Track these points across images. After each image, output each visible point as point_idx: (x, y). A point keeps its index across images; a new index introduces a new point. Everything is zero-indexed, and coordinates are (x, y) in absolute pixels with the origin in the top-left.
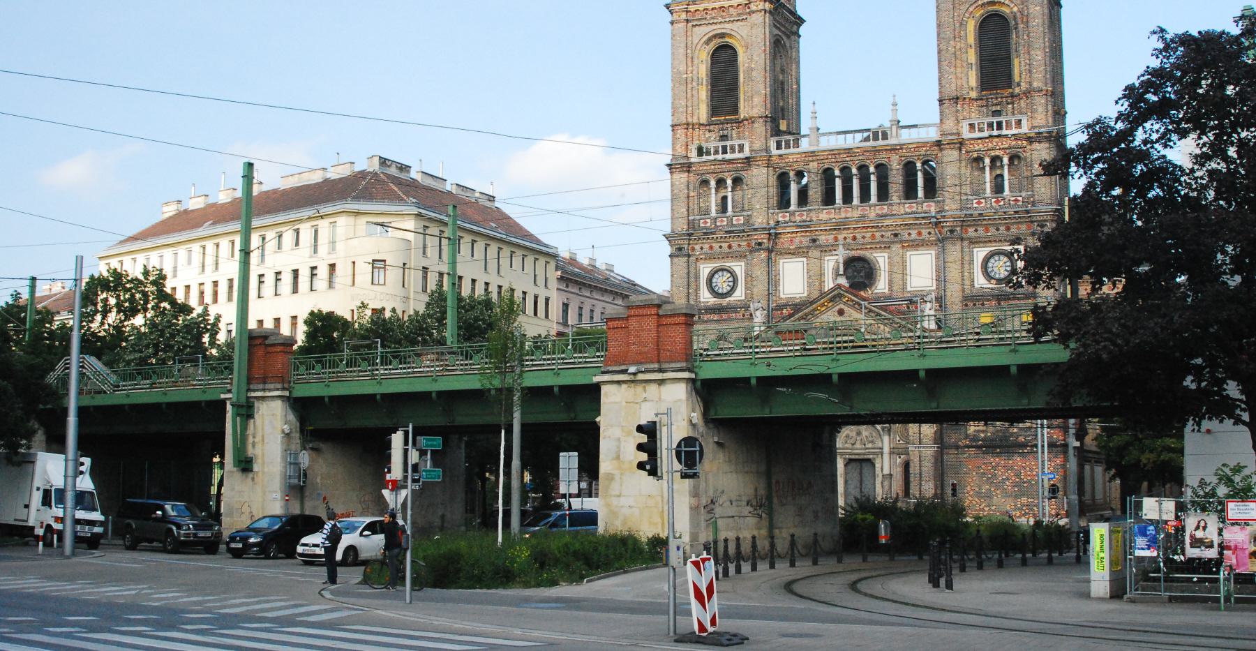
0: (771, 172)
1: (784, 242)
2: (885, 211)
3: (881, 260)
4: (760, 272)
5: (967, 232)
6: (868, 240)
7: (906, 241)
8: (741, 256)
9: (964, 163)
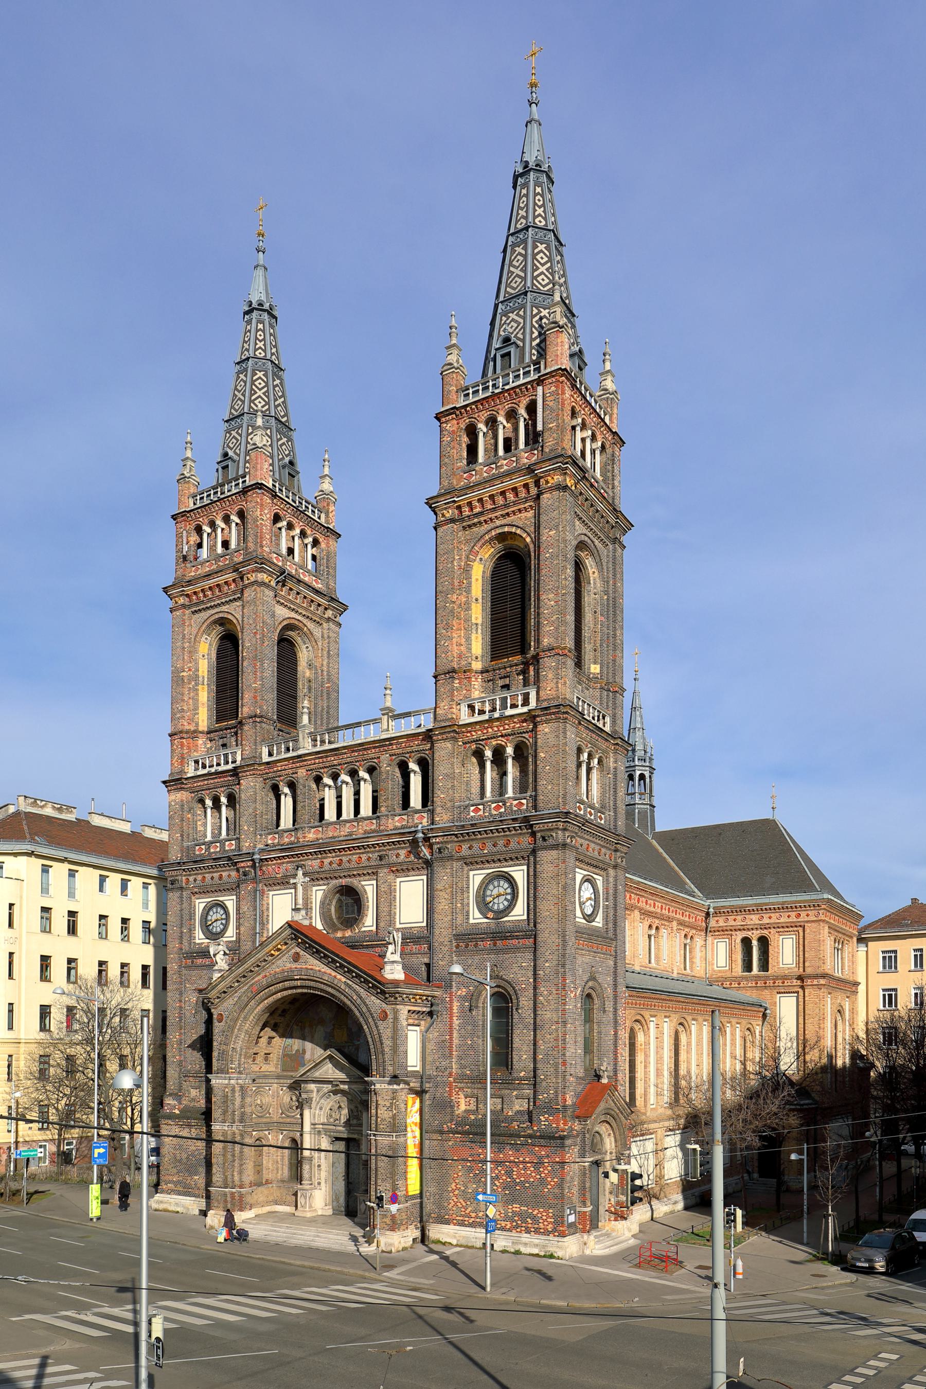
3: (369, 888)
6: (353, 864)
7: (394, 864)
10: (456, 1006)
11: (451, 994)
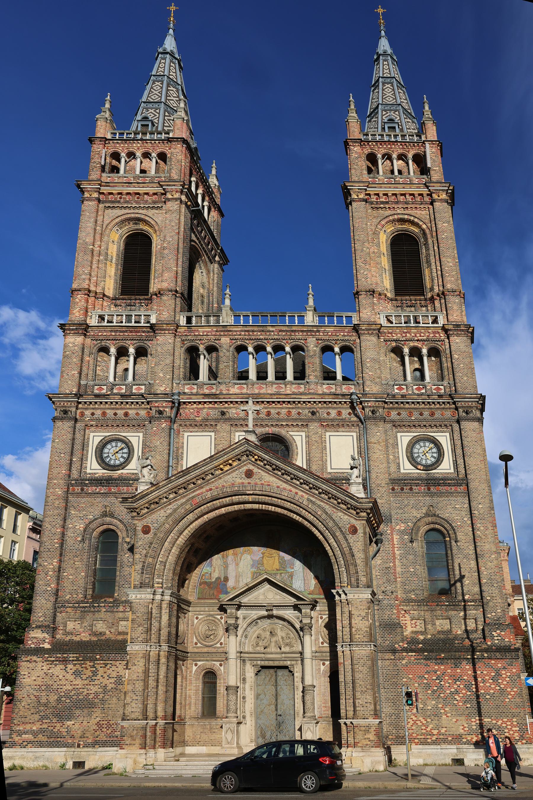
0: (178, 344)
1: (187, 411)
2: (302, 390)
4: (159, 442)
5: (389, 414)
7: (325, 420)
8: (138, 425)
9: (383, 350)
10: (396, 537)
11: (391, 527)
